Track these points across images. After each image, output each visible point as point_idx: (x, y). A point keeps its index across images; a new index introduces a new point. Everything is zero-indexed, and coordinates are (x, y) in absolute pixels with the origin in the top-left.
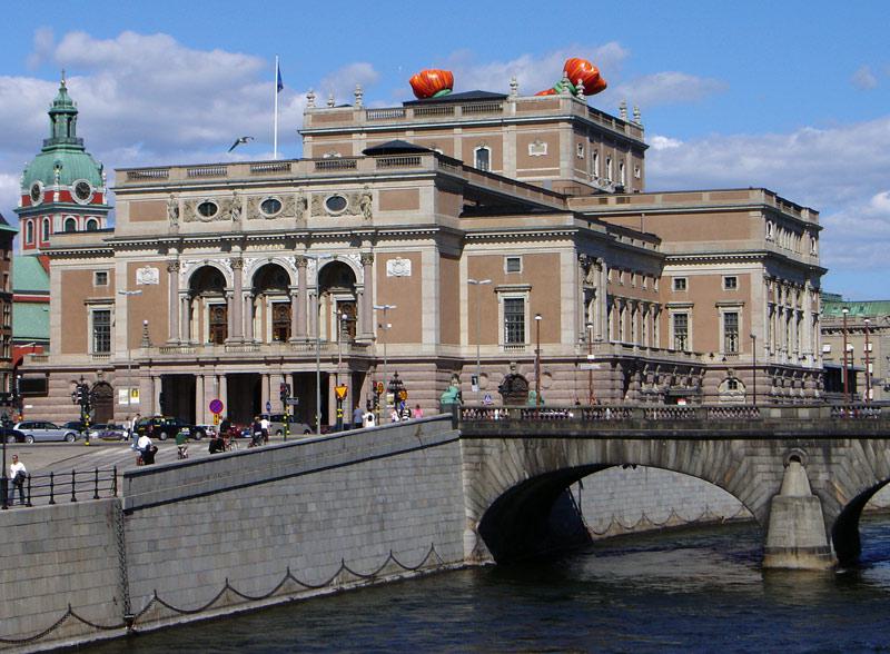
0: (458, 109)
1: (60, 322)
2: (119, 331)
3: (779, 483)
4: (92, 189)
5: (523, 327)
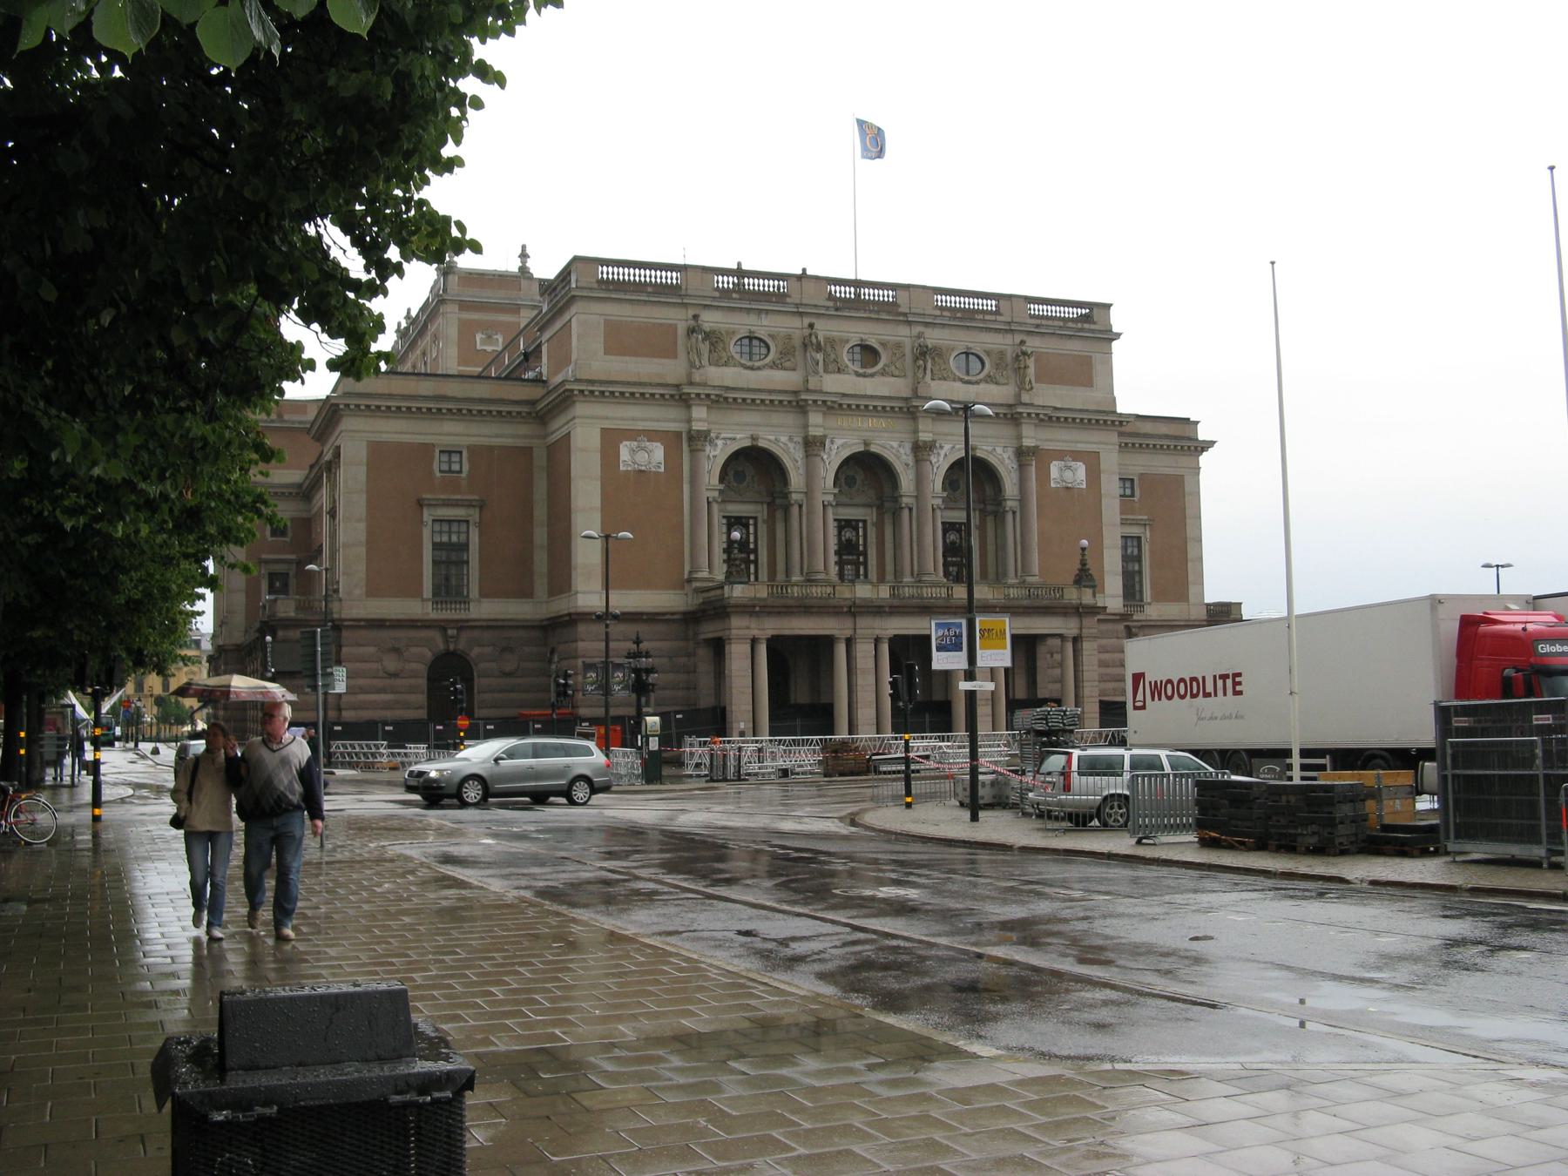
1: (363, 538)
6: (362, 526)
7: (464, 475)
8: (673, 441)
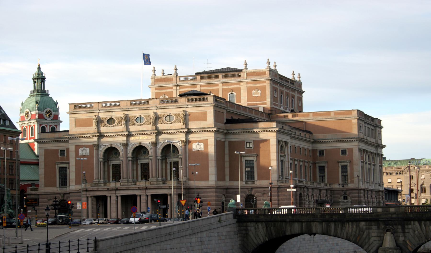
0: (220, 76)
1: (43, 173)
2: (72, 175)
3: (381, 242)
4: (53, 113)
5: (254, 172)
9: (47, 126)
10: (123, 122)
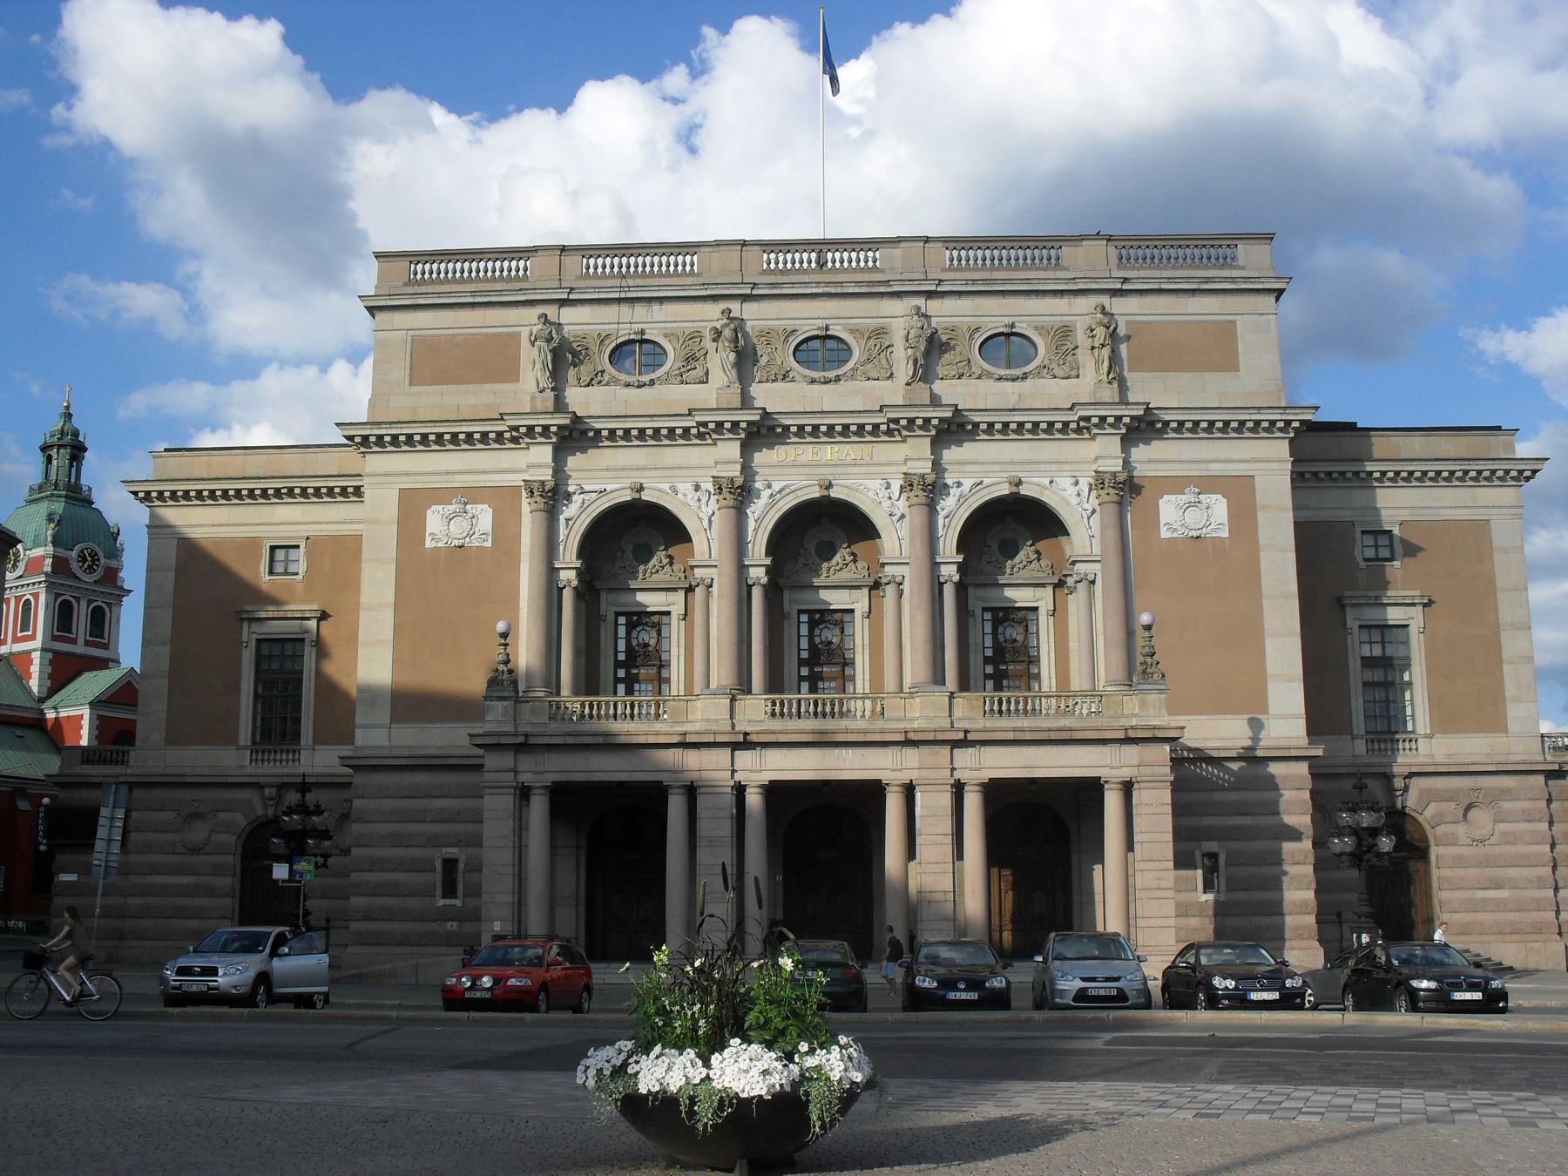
1: (166, 666)
4: (103, 560)
6: (167, 649)
7: (300, 577)
8: (502, 499)
9: (78, 599)
10: (720, 361)
